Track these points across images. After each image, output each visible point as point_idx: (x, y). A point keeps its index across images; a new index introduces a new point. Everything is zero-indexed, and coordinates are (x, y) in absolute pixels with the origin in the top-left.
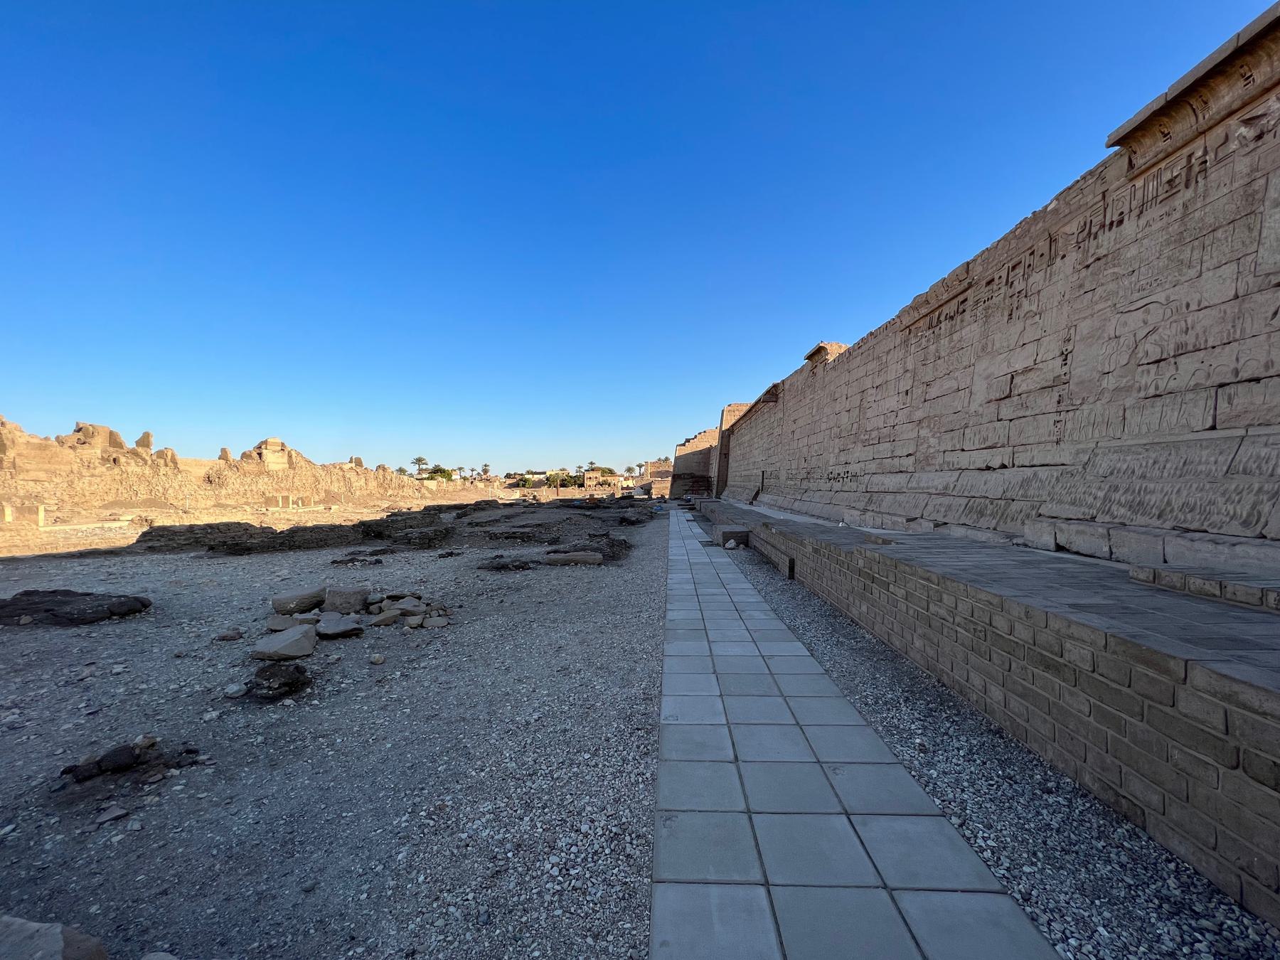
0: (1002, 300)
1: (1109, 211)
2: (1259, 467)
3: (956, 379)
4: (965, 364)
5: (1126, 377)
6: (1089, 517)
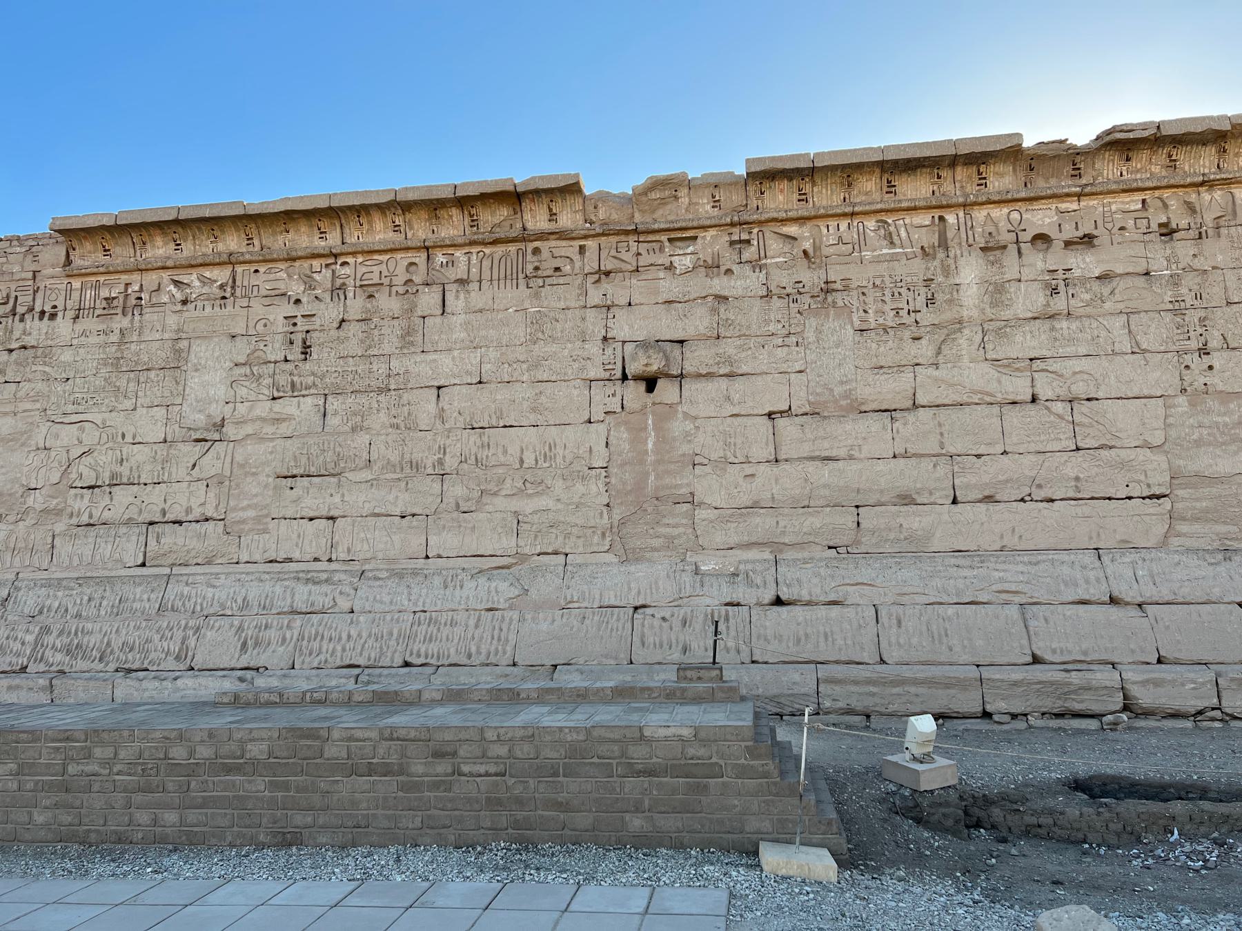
1: (40, 295)
2: (184, 604)
5: (56, 498)
6: (19, 667)
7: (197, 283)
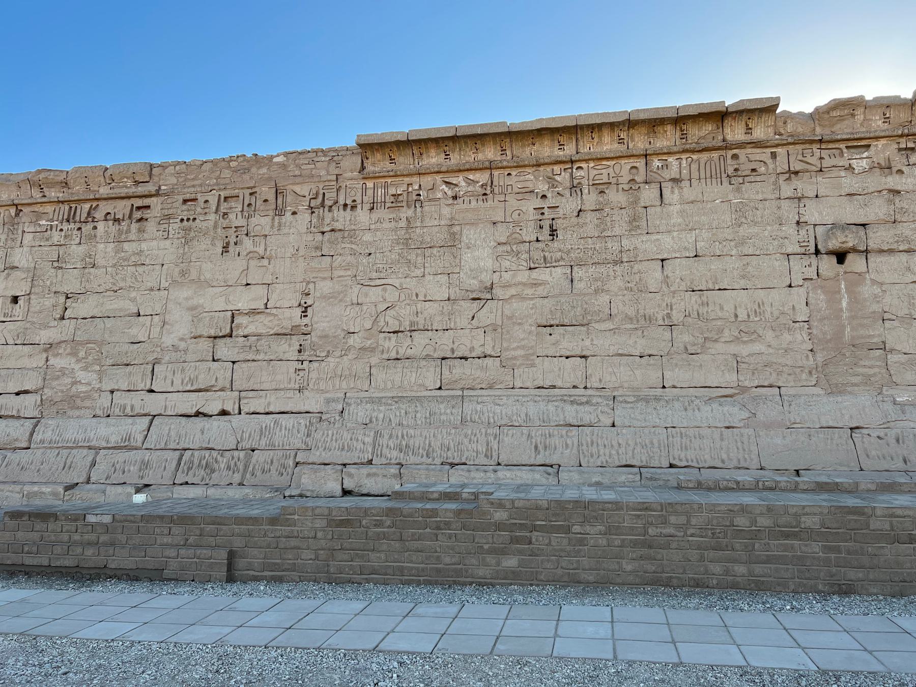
0: (211, 228)
1: (342, 192)
2: (479, 418)
3: (133, 300)
4: (149, 285)
6: (366, 460)
7: (463, 184)
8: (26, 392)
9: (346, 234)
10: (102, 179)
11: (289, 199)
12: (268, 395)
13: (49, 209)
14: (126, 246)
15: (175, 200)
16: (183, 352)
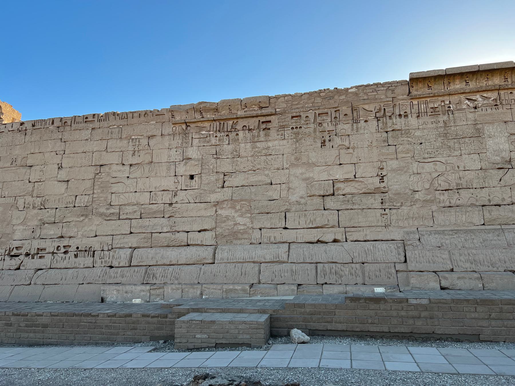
1: (397, 107)
3: (267, 175)
4: (276, 166)
5: (429, 195)
7: (480, 99)
8: (205, 230)
9: (403, 132)
10: (240, 106)
11: (361, 113)
12: (365, 230)
13: (207, 124)
14: (258, 145)
15: (286, 117)
16: (304, 205)
